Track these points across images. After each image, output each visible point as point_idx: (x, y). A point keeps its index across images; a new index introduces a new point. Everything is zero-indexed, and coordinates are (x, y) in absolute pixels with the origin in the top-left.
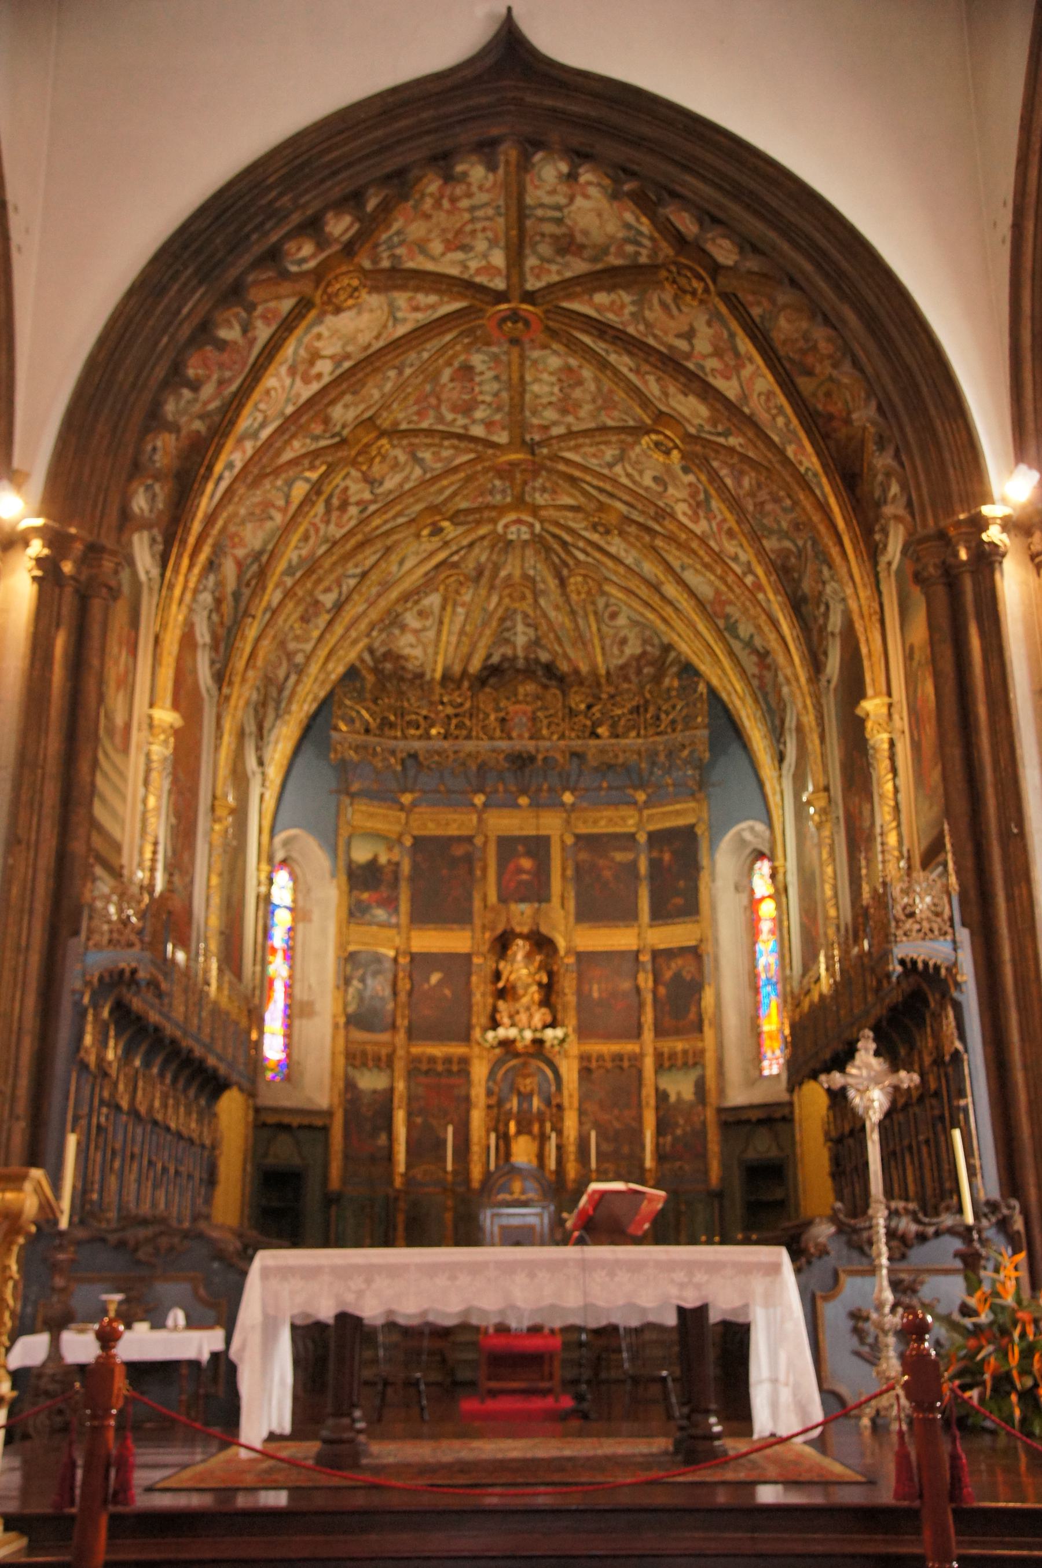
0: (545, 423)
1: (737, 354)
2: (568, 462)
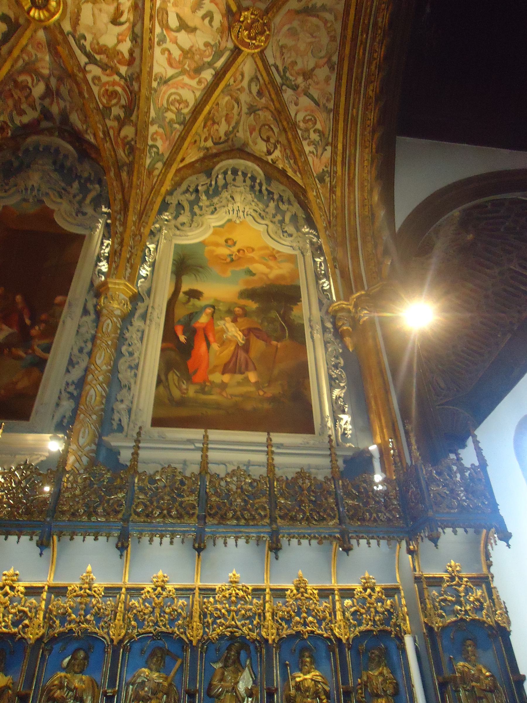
1: (198, 70)
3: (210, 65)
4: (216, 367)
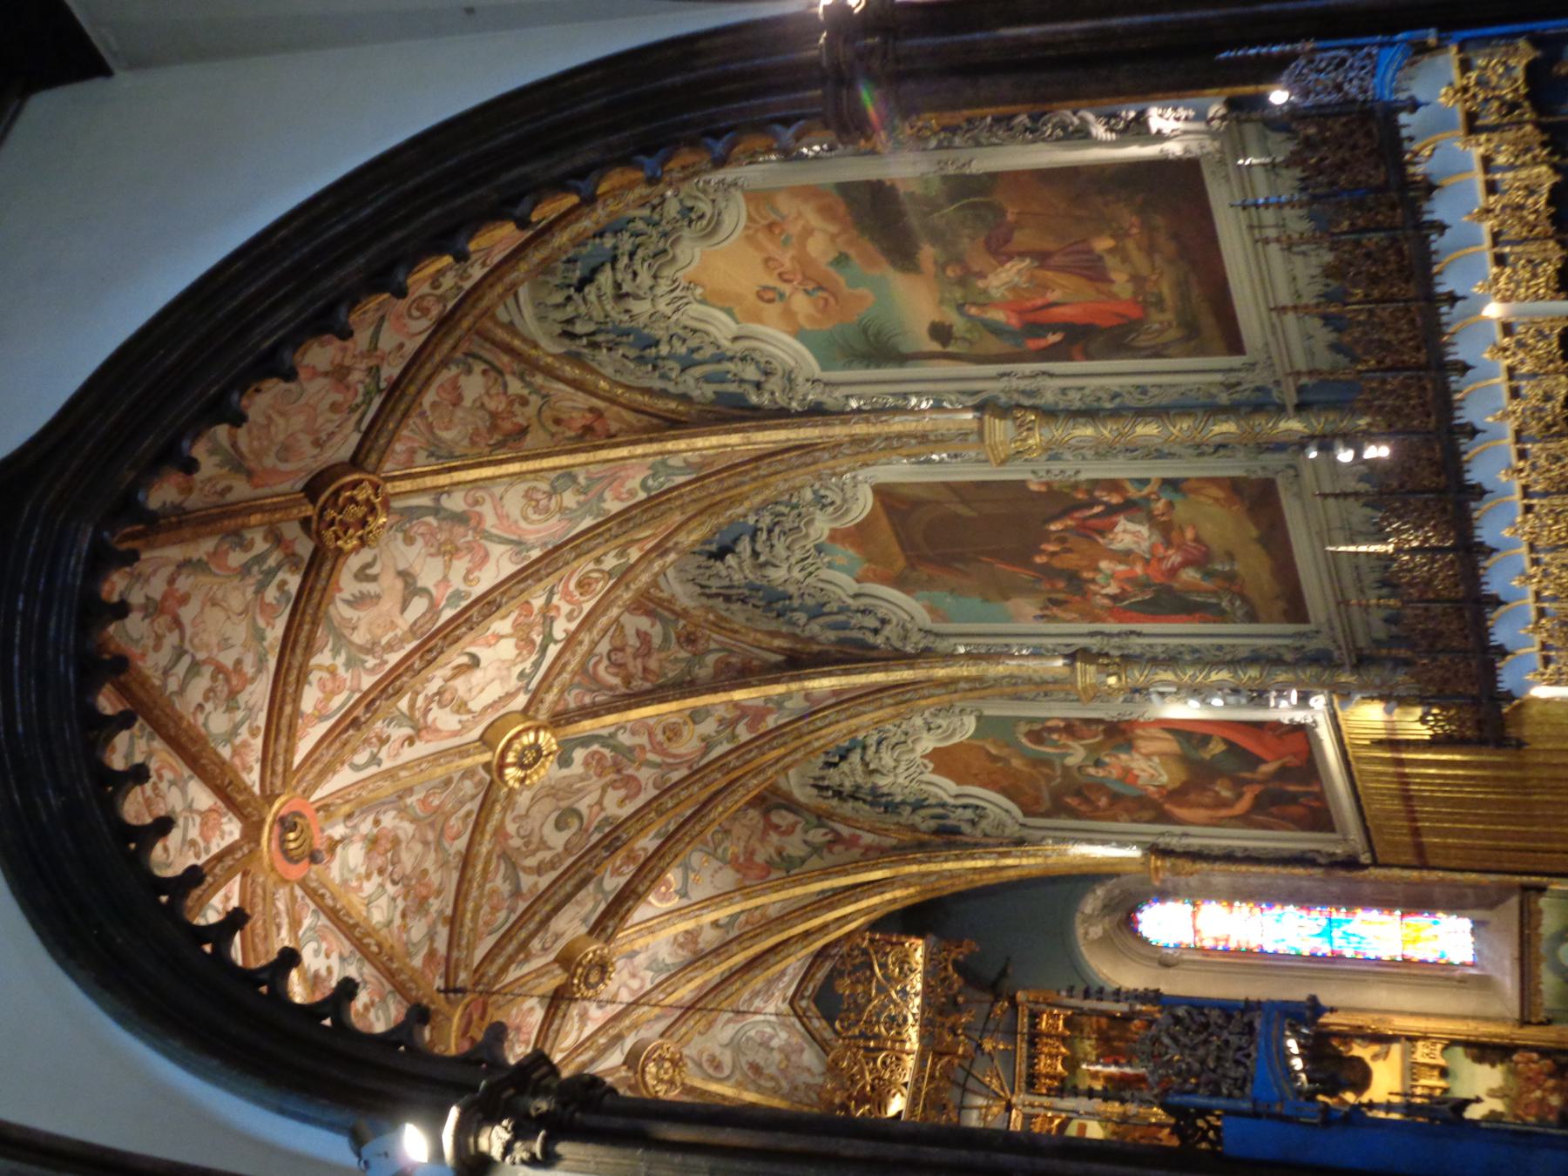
0: (425, 951)
1: (461, 519)
2: (489, 957)
3: (436, 511)
4: (1099, 291)
